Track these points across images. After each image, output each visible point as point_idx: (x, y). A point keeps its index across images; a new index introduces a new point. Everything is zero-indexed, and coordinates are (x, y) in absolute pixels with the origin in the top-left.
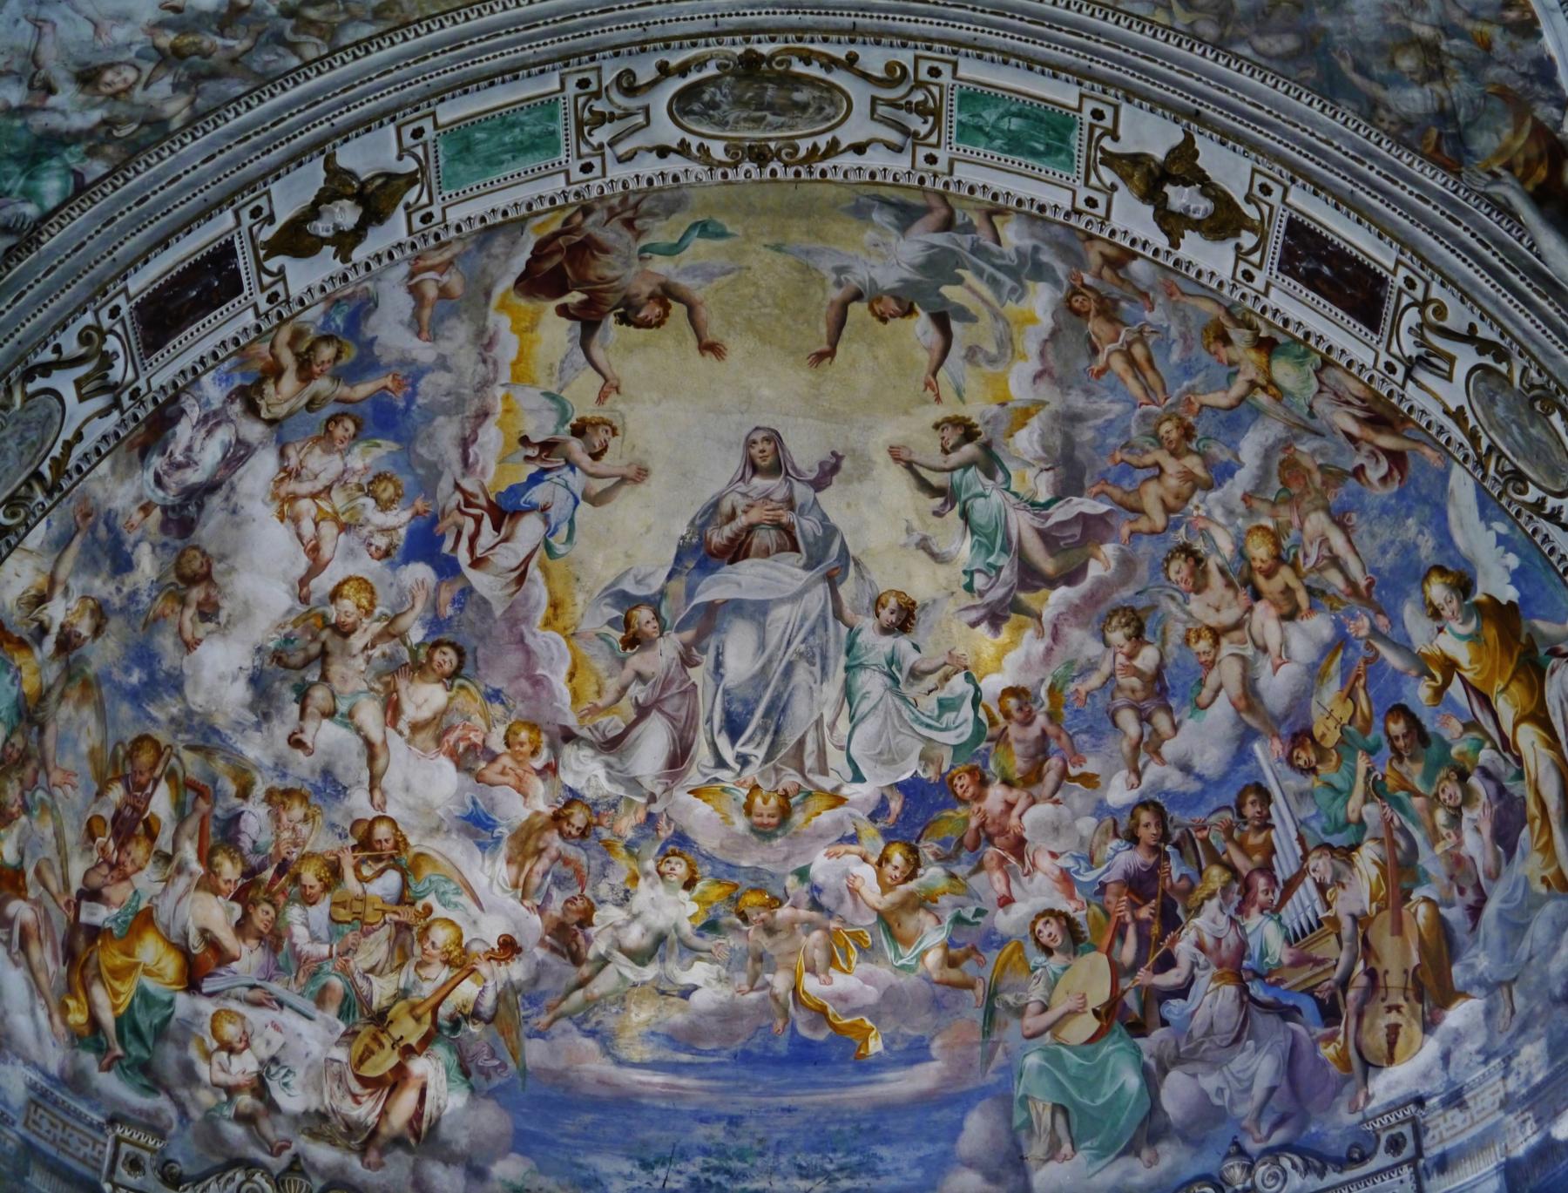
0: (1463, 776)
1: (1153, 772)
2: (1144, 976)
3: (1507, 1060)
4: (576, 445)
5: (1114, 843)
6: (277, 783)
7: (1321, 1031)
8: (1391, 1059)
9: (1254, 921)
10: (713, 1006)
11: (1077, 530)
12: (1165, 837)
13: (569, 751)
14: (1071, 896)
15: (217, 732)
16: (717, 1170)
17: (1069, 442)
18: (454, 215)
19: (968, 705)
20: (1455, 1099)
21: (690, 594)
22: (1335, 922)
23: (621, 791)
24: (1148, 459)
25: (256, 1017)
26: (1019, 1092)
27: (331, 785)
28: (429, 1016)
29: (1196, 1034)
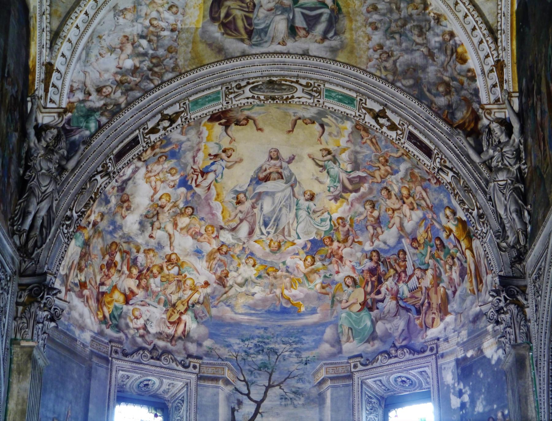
0: (453, 258)
1: (376, 243)
2: (373, 295)
3: (459, 333)
4: (223, 155)
5: (366, 260)
6: (147, 248)
7: (416, 316)
8: (432, 327)
9: (401, 285)
11: (358, 179)
12: (379, 260)
13: (222, 232)
14: (355, 273)
15: (131, 237)
16: (261, 342)
17: (356, 158)
18: (192, 117)
19: (328, 220)
20: (446, 340)
21: (254, 190)
22: (421, 288)
23: (236, 242)
24: (377, 165)
25: (143, 309)
26: (340, 323)
27: (160, 246)
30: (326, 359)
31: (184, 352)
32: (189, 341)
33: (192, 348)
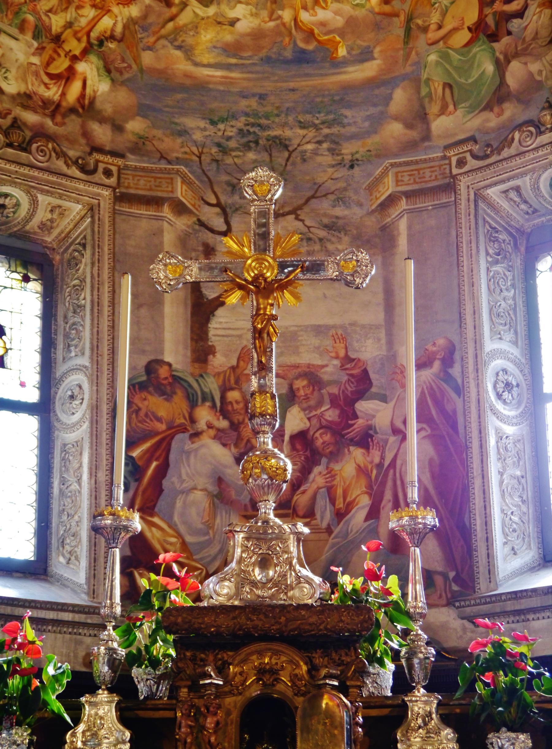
10: (249, 30)
16: (253, 125)
26: (425, 76)
28: (85, 39)
29: (527, 39)
30: (396, 156)
31: (83, 141)
32: (93, 118)
33: (101, 133)
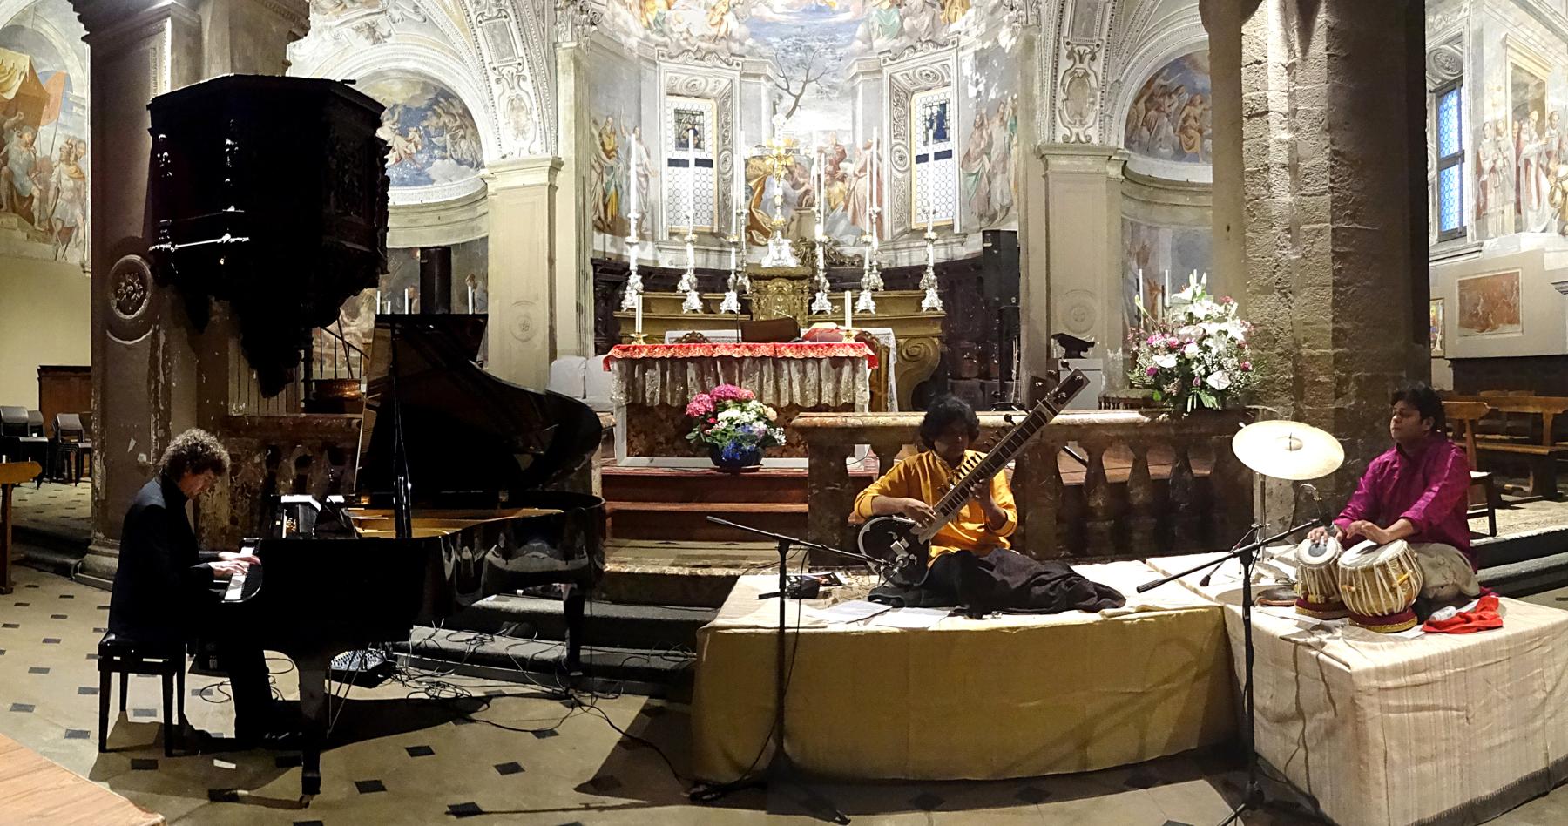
20: (967, 33)
33: (735, 47)
